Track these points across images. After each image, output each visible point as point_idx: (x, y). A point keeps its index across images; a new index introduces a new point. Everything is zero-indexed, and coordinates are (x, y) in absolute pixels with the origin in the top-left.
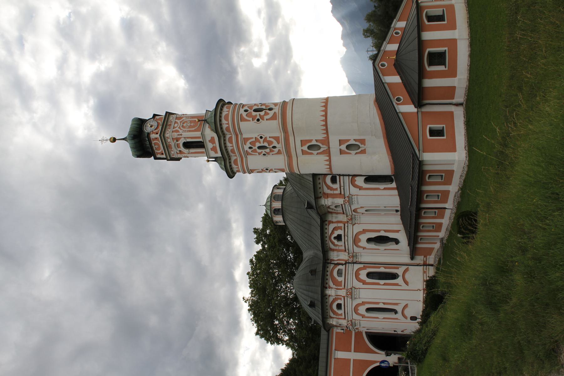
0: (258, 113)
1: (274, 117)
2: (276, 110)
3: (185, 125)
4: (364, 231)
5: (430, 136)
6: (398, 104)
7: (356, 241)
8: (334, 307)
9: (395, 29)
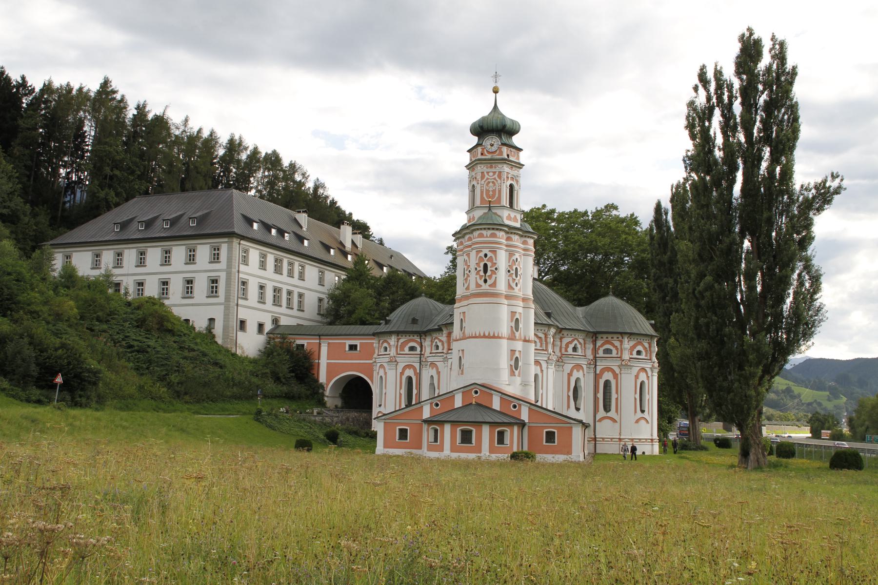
0: (482, 268)
1: (478, 286)
2: (485, 287)
3: (491, 184)
4: (439, 373)
5: (406, 430)
6: (431, 404)
7: (433, 365)
8: (385, 345)
9: (520, 405)
